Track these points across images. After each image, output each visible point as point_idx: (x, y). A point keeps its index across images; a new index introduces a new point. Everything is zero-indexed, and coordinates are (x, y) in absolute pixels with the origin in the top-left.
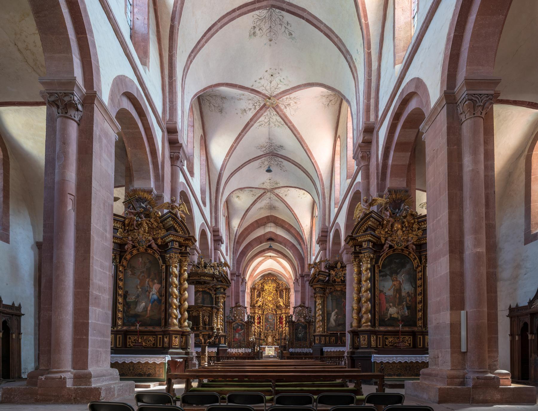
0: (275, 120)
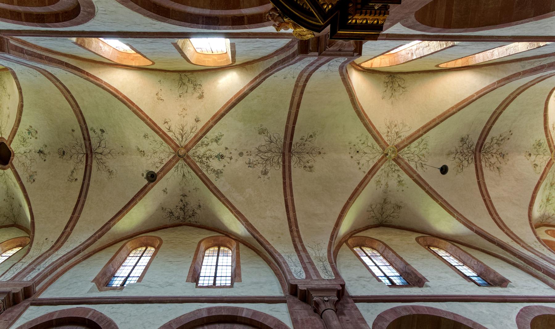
0: (416, 149)
